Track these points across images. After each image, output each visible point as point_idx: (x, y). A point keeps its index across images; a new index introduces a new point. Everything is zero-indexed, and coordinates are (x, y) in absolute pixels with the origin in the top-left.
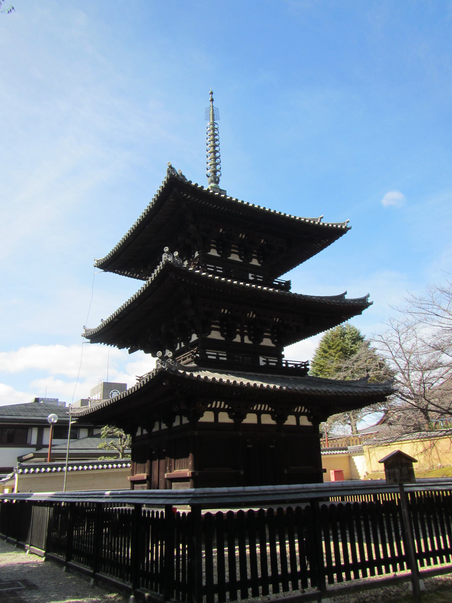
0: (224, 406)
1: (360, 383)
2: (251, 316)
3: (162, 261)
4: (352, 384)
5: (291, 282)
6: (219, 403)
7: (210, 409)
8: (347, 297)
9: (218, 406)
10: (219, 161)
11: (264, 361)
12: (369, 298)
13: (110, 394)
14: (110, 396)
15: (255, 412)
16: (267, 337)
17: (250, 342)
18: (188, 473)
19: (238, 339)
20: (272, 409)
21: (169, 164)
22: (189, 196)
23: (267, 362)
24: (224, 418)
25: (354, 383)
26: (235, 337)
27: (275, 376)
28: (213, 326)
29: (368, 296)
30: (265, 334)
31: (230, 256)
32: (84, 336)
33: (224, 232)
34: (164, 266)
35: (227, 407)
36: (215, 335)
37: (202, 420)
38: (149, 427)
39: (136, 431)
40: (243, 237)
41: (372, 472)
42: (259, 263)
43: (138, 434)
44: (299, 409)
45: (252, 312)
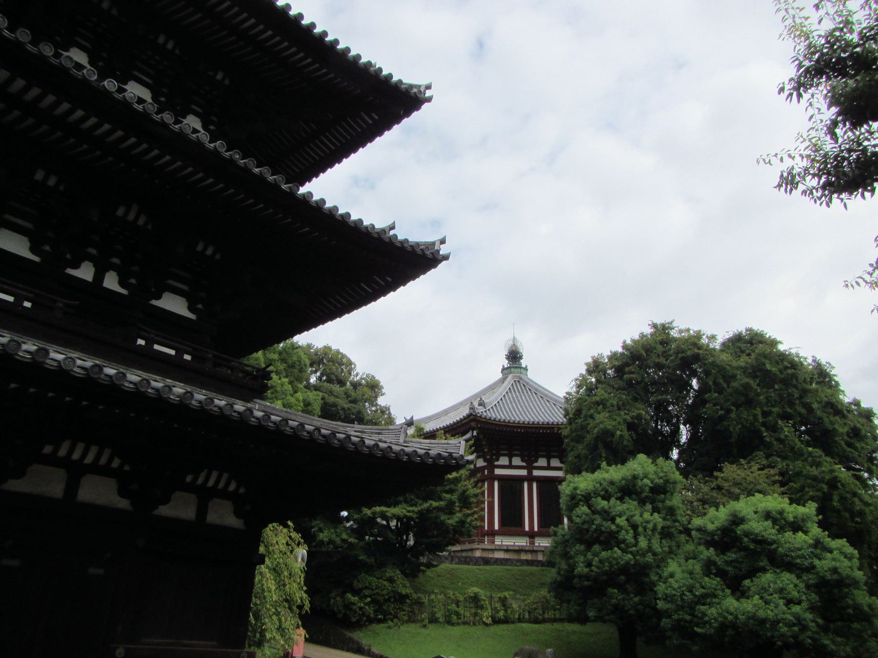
2: (131, 217)
15: (66, 463)
20: (121, 466)
26: (76, 266)
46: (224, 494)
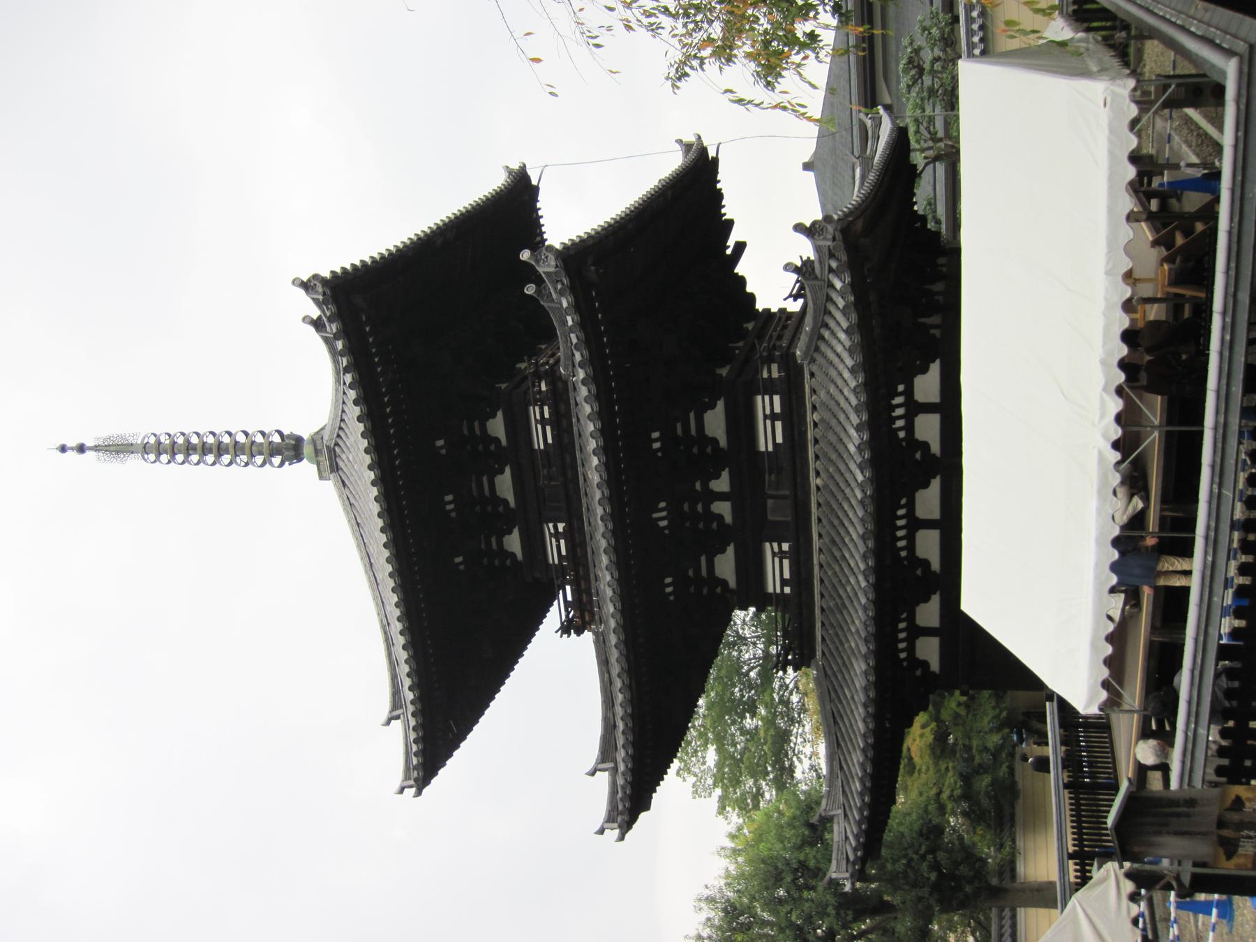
17: (725, 475)
19: (723, 509)
26: (720, 518)
36: (726, 566)
37: (935, 666)
45: (655, 515)
46: (909, 392)
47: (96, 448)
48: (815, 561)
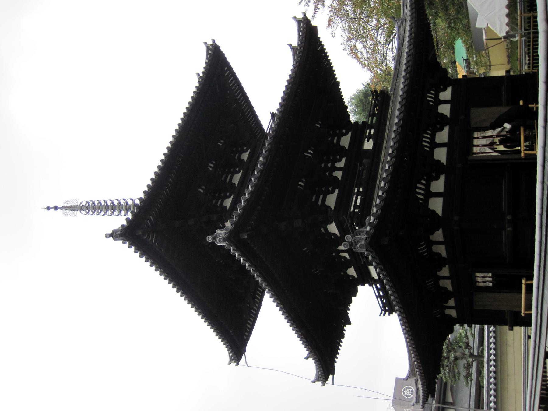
0: (422, 184)
1: (400, 27)
3: (224, 246)
4: (401, 37)
5: (273, 113)
6: (418, 191)
7: (426, 202)
8: (295, 43)
9: (422, 192)
10: (124, 201)
11: (368, 141)
12: (298, 17)
13: (407, 397)
14: (408, 397)
16: (339, 141)
18: (508, 229)
19: (339, 174)
21: (108, 236)
22: (151, 217)
23: (370, 137)
24: (439, 185)
25: (401, 34)
26: (336, 177)
27: (387, 127)
28: (320, 203)
29: (295, 18)
30: (335, 141)
31: (235, 184)
32: (325, 382)
33: (204, 187)
34: (231, 244)
35: (423, 182)
36: (331, 200)
38: (446, 295)
39: (450, 316)
40: (212, 165)
41: (508, 63)
42: (246, 151)
43: (453, 313)
44: (430, 98)
45: (306, 154)
47: (62, 208)
48: (380, 166)
